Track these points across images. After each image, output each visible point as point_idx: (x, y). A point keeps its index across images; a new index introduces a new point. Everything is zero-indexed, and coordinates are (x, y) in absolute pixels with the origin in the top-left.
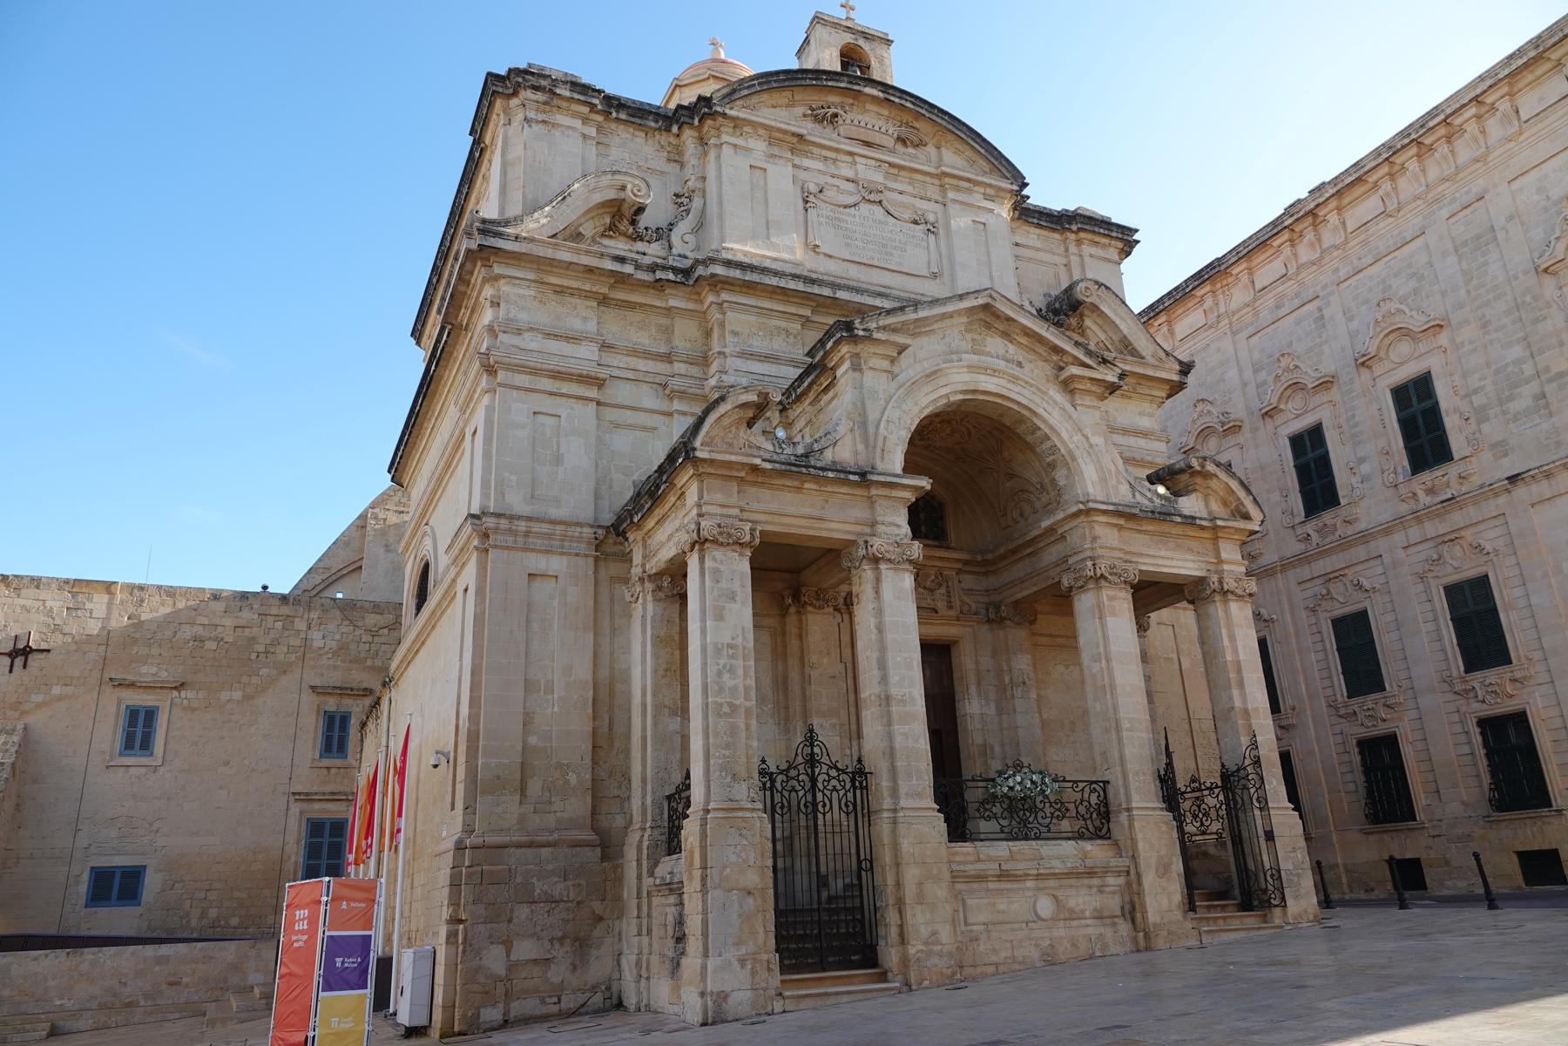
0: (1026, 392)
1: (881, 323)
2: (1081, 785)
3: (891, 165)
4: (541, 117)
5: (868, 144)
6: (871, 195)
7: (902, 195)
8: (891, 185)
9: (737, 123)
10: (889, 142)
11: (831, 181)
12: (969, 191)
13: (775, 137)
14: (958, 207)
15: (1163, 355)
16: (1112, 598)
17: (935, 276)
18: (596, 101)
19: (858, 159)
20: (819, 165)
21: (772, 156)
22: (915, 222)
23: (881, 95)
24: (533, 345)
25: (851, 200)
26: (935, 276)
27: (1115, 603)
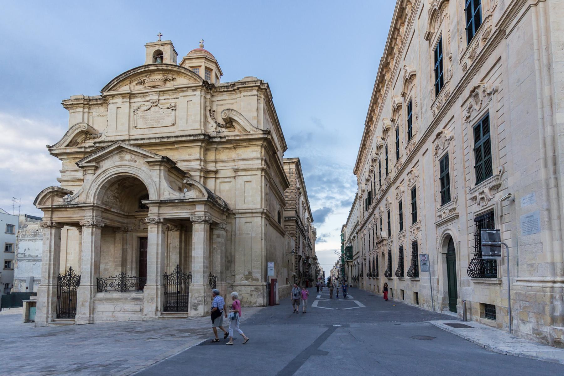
0: (134, 170)
3: (160, 91)
5: (154, 87)
6: (155, 104)
7: (166, 100)
8: (161, 98)
9: (113, 96)
11: (142, 103)
12: (187, 91)
13: (123, 95)
15: (255, 129)
16: (151, 228)
17: (174, 125)
19: (149, 93)
20: (139, 99)
21: (123, 102)
22: (168, 108)
25: (147, 108)
26: (174, 125)
27: (153, 229)
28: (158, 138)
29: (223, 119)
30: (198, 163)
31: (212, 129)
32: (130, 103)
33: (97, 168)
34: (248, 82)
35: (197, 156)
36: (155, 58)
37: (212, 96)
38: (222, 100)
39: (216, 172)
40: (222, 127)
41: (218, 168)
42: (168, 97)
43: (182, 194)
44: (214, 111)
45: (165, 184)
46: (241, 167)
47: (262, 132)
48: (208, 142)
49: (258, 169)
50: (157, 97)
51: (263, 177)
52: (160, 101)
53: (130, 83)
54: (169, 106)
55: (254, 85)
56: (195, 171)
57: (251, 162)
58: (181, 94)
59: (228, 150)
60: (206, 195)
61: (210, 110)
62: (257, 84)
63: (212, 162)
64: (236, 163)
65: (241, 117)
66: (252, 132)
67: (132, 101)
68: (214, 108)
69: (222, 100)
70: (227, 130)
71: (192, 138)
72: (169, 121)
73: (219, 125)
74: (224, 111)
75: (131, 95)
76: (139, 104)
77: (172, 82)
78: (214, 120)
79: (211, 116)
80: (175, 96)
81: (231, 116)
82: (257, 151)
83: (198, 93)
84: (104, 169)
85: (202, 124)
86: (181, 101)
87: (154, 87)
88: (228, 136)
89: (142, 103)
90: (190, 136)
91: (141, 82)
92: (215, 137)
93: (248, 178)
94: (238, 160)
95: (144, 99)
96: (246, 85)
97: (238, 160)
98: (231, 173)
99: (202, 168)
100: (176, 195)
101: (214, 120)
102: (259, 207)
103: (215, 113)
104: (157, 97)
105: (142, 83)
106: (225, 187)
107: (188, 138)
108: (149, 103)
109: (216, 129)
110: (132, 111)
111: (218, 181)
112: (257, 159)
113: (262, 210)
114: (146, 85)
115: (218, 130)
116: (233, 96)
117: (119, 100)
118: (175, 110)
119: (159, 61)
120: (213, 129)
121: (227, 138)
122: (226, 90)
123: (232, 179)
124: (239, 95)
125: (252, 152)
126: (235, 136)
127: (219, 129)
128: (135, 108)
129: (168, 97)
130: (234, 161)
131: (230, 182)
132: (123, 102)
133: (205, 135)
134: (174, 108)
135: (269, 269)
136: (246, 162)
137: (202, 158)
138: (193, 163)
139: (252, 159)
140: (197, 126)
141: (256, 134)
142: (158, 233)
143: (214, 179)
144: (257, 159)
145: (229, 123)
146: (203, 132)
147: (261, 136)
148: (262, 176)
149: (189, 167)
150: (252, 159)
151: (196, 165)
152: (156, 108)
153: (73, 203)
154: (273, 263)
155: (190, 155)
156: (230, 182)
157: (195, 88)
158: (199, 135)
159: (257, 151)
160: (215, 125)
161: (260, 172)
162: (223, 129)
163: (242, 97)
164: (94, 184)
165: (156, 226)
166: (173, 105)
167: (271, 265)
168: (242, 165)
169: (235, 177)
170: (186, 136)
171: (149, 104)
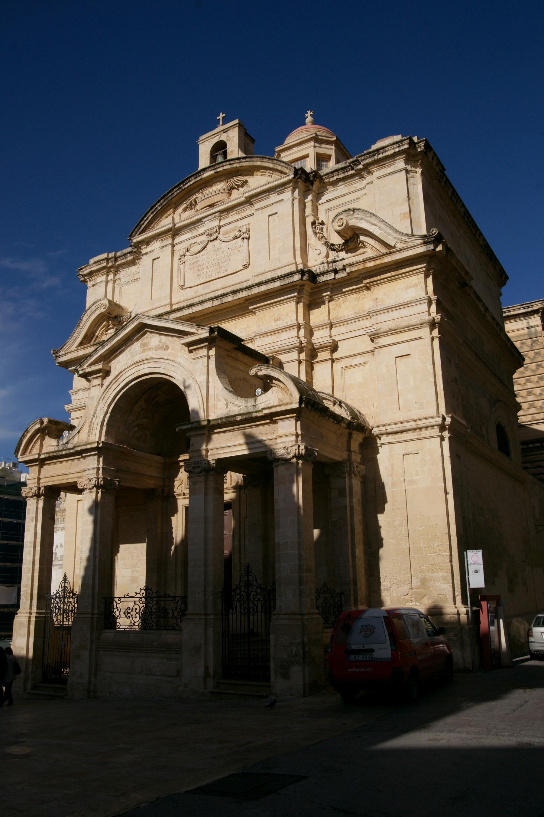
1: (89, 362)
2: (178, 599)
3: (221, 212)
4: (93, 283)
5: (212, 206)
7: (233, 223)
8: (222, 223)
9: (147, 241)
10: (224, 196)
11: (193, 241)
14: (260, 211)
15: (405, 238)
17: (246, 267)
18: (105, 264)
21: (162, 247)
22: (236, 238)
23: (213, 172)
24: (82, 397)
25: (199, 247)
26: (246, 267)
28: (217, 298)
29: (338, 232)
30: (294, 332)
31: (316, 260)
32: (173, 246)
33: (107, 373)
34: (383, 148)
35: (292, 320)
36: (213, 157)
37: (319, 196)
38: (336, 198)
39: (334, 348)
40: (337, 251)
41: (337, 338)
42: (236, 217)
43: (251, 402)
44: (322, 223)
45: (217, 386)
46: (384, 327)
47: (421, 241)
48: (310, 288)
49: (421, 325)
50: (216, 223)
51: (436, 342)
52: (222, 230)
53: (174, 213)
54: (237, 234)
55: (397, 150)
56: (288, 351)
57: (404, 312)
58: (257, 206)
59: (354, 296)
60: (296, 395)
61: (313, 223)
62: (402, 148)
63: (321, 327)
64: (373, 320)
65: (373, 220)
66: (399, 246)
67: (177, 240)
68: (322, 217)
69: (336, 198)
70: (350, 255)
71: (277, 284)
72: (237, 263)
73: (332, 247)
74: (337, 216)
75: (175, 232)
76: (186, 244)
77: (241, 189)
78: (323, 241)
79: (316, 234)
80: (248, 213)
81: (353, 222)
82: (416, 285)
83: (287, 195)
84: (117, 373)
85: (298, 253)
86: (256, 219)
87: (212, 206)
88: (351, 265)
89: (193, 241)
90: (273, 280)
91: (191, 205)
92: (323, 274)
93: (402, 349)
94: (377, 312)
95: (195, 233)
96: (381, 156)
97: (377, 312)
98: (366, 344)
99: (301, 342)
100: (238, 406)
101: (323, 241)
102: (433, 411)
103: (325, 227)
104: (216, 223)
105: (191, 206)
106: (355, 377)
107: (272, 286)
108: (204, 238)
109: (327, 256)
110: (176, 258)
111: (338, 366)
112: (418, 301)
113: (440, 419)
114: (198, 207)
115: (330, 259)
116: (358, 184)
117: (156, 245)
118: (249, 238)
119: (220, 159)
120: (321, 258)
121: (348, 270)
122: (341, 176)
123: (367, 357)
124: (369, 178)
125: (407, 288)
126: (364, 261)
127: (333, 255)
128: (181, 253)
129: (236, 217)
130: (369, 315)
131: (364, 364)
132: (162, 247)
133: (302, 273)
134: (246, 236)
135: (471, 569)
136: (395, 314)
137: (301, 321)
138: (284, 335)
139: (406, 305)
140: (288, 258)
141: (408, 248)
142: (206, 494)
143: (330, 362)
144: (418, 301)
145: (352, 238)
146: (300, 267)
147: (422, 249)
148: (433, 339)
149: (277, 346)
150: (406, 305)
151: (290, 338)
152: (216, 242)
153: (70, 446)
154: (479, 553)
155: (279, 319)
156: (364, 364)
157: (279, 188)
158: (291, 274)
159: (416, 285)
160: (324, 249)
161: (428, 329)
162: (342, 254)
163: (376, 182)
164: (101, 405)
165: (203, 479)
166: (244, 230)
167: (475, 558)
168: (385, 321)
169: (373, 351)
170: (267, 282)
171: (204, 238)
